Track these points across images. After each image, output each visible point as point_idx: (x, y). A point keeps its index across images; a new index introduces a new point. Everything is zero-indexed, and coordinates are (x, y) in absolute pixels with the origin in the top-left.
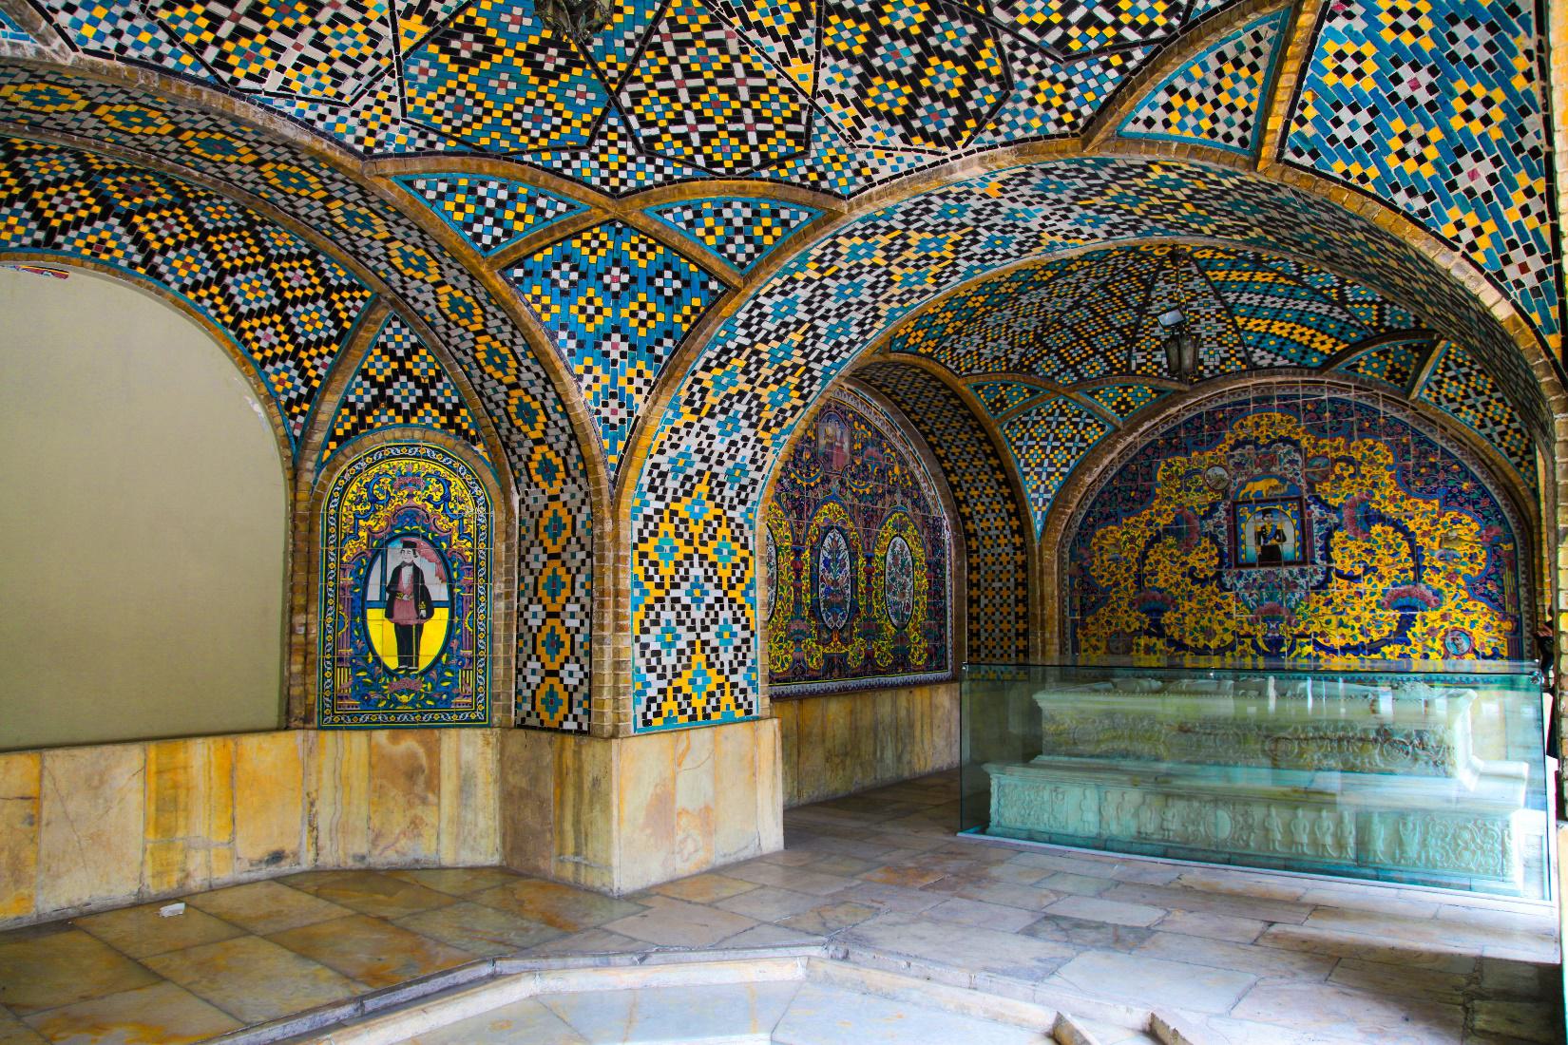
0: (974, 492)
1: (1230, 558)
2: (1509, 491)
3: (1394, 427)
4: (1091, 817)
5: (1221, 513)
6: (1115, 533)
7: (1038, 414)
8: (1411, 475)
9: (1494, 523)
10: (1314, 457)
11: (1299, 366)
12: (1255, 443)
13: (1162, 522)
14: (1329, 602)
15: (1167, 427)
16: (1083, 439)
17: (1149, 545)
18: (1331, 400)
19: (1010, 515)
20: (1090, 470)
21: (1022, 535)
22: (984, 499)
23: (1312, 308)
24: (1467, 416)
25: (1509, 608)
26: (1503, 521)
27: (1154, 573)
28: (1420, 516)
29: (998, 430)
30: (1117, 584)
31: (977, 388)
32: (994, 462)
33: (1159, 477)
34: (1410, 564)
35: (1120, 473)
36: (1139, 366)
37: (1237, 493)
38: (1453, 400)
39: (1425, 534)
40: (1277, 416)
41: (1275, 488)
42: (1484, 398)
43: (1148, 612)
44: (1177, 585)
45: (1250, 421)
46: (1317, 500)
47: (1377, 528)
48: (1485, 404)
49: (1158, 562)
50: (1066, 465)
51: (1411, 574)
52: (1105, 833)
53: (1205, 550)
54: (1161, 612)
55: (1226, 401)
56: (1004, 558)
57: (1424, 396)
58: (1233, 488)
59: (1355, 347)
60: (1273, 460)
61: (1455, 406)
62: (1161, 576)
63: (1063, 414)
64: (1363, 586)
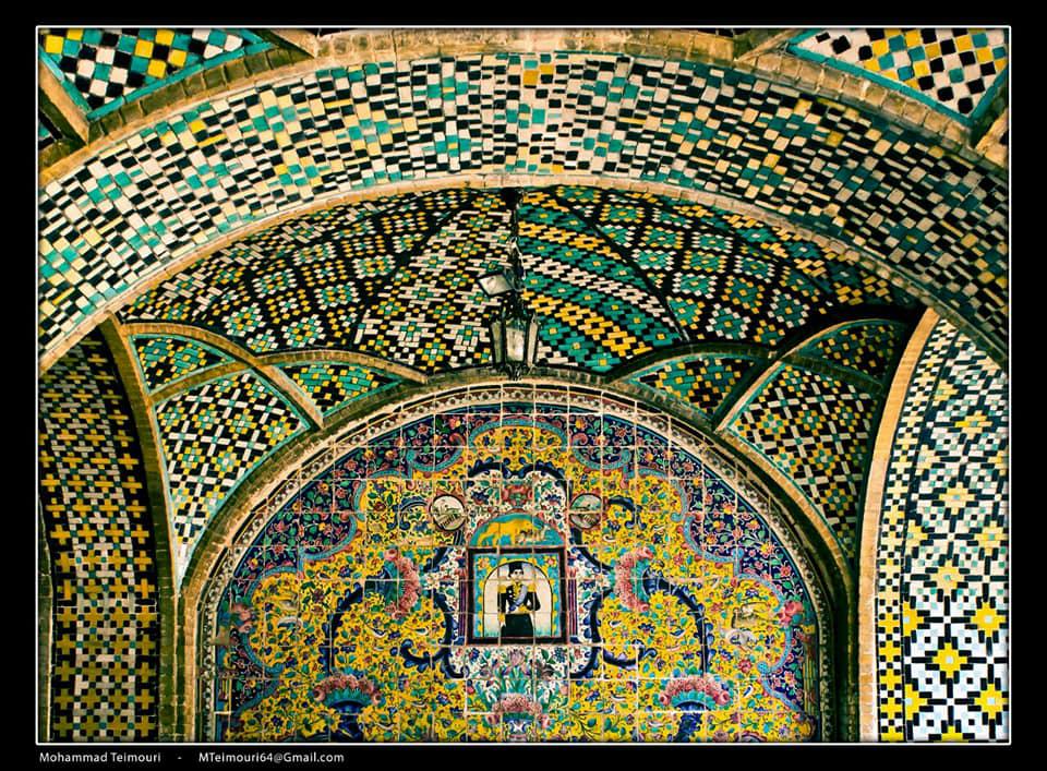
0: (80, 507)
1: (462, 629)
2: (818, 555)
3: (682, 466)
5: (451, 565)
6: (293, 580)
7: (211, 393)
8: (701, 529)
9: (796, 597)
11: (581, 368)
13: (363, 573)
14: (596, 695)
15: (378, 433)
16: (262, 439)
17: (345, 605)
18: (608, 419)
19: (137, 547)
20: (262, 484)
21: (153, 580)
22: (98, 520)
23: (623, 293)
24: (785, 461)
25: (809, 708)
26: (805, 597)
28: (711, 579)
29: (151, 414)
31: (140, 342)
32: (129, 461)
33: (364, 504)
34: (697, 646)
35: (303, 495)
36: (366, 338)
40: (537, 433)
42: (811, 440)
43: (339, 706)
45: (499, 436)
46: (584, 552)
47: (658, 597)
50: (232, 476)
51: (697, 660)
53: (427, 617)
54: (357, 706)
55: (465, 403)
56: (119, 616)
57: (734, 428)
58: (470, 529)
59: (660, 353)
60: (527, 495)
61: (772, 445)
62: (359, 650)
63: (244, 397)
64: (636, 674)
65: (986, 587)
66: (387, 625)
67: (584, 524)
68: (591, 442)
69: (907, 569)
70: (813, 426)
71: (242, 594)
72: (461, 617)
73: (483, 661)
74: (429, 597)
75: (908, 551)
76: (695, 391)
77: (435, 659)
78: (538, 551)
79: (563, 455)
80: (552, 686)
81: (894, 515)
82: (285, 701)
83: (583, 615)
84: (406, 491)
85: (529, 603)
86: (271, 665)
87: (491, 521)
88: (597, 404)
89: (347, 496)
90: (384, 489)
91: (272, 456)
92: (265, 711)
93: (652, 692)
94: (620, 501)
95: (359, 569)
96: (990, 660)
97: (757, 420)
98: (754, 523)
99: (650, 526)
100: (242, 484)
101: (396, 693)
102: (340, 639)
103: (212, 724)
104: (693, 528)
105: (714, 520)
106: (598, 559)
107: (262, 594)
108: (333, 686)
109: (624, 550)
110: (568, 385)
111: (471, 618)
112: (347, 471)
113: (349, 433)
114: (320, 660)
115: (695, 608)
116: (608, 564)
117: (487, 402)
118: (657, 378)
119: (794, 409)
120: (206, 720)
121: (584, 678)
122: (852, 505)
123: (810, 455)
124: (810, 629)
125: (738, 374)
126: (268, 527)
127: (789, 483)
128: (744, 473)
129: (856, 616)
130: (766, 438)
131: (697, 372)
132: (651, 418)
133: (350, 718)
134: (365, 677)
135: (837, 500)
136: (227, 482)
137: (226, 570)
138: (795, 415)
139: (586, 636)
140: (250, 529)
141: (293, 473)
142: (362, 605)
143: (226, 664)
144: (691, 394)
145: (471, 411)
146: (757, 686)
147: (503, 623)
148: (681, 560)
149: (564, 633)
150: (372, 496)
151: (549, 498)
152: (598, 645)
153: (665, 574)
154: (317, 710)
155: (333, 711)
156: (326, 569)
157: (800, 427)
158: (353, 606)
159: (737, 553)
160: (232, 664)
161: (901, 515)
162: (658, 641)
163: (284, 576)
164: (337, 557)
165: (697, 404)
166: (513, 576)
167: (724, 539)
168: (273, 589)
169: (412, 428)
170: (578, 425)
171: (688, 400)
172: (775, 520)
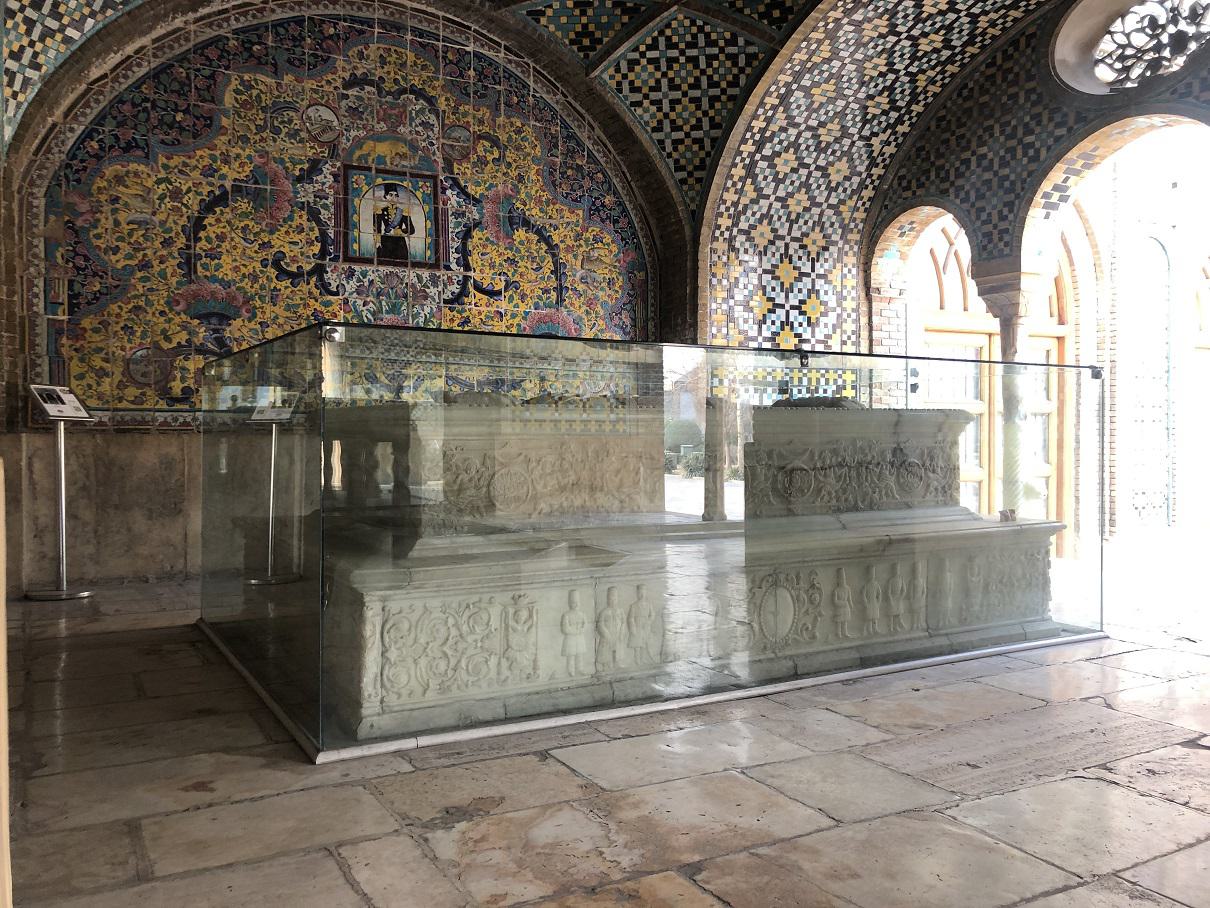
1: (337, 246)
3: (541, 110)
4: (581, 643)
5: (326, 177)
10: (453, 126)
12: (378, 84)
13: (231, 174)
15: (243, 23)
17: (208, 207)
18: (476, 54)
20: (108, 50)
26: (638, 247)
27: (213, 255)
28: (566, 223)
30: (145, 265)
33: (229, 99)
34: (553, 283)
35: (155, 75)
37: (350, 153)
38: (638, 90)
39: (569, 249)
40: (411, 57)
41: (403, 156)
43: (204, 317)
44: (254, 278)
45: (373, 50)
46: (456, 183)
47: (520, 234)
48: (674, 103)
49: (221, 238)
50: (78, 25)
51: (554, 295)
52: (608, 674)
54: (225, 318)
57: (606, 76)
58: (344, 144)
61: (638, 97)
62: (226, 259)
64: (503, 305)
65: (787, 246)
66: (256, 234)
67: (456, 155)
68: (461, 75)
69: (735, 224)
70: (684, 80)
71: (78, 181)
72: (337, 233)
73: (359, 280)
74: (302, 209)
75: (740, 208)
76: (577, 33)
77: (310, 273)
78: (412, 175)
79: (436, 83)
80: (427, 310)
81: (739, 172)
82: (137, 308)
83: (456, 244)
84: (276, 93)
85: (404, 227)
86: (119, 266)
87: (366, 138)
88: (468, 39)
89: (209, 87)
90: (252, 87)
91: (129, 13)
92: (113, 318)
93: (516, 321)
94: (486, 137)
95: (225, 170)
96: (787, 307)
97: (631, 70)
98: (600, 175)
99: (514, 165)
100: (89, 40)
101: (268, 308)
102: (203, 244)
103: (42, 328)
104: (551, 173)
105: (568, 168)
106: (469, 190)
107: (105, 184)
108: (196, 296)
109: (491, 185)
110: (441, 14)
111: (346, 235)
112: (208, 58)
113: (209, 16)
114: (179, 266)
115: (552, 248)
116: (477, 196)
117: (360, 14)
118: (543, 13)
119: (671, 61)
120: (33, 325)
121: (456, 305)
122: (702, 160)
123: (673, 109)
124: (641, 275)
125: (625, 19)
126: (111, 104)
127: (646, 136)
128: (593, 129)
129: (696, 261)
130: (634, 89)
131: (583, 13)
132: (515, 62)
133: (216, 331)
134: (233, 288)
135: (689, 155)
136: (71, 32)
137: (56, 150)
138: (670, 67)
139: (458, 264)
140: (87, 105)
141: (142, 48)
142: (227, 210)
143: (60, 260)
144: (572, 36)
145: (345, 21)
146: (601, 322)
147: (379, 244)
148: (541, 202)
149: (437, 259)
150: (237, 91)
151: (422, 124)
152: (469, 274)
153: (527, 213)
154: (177, 320)
155: (196, 322)
156: (185, 165)
157: (671, 80)
158: (217, 210)
159: (586, 203)
160: (67, 262)
161: (743, 173)
162: (521, 275)
163: (133, 166)
164: (199, 153)
165: (575, 48)
166: (388, 197)
167: (576, 186)
168: (119, 180)
169: (281, 25)
170: (450, 56)
171: (567, 42)
172: (617, 176)
